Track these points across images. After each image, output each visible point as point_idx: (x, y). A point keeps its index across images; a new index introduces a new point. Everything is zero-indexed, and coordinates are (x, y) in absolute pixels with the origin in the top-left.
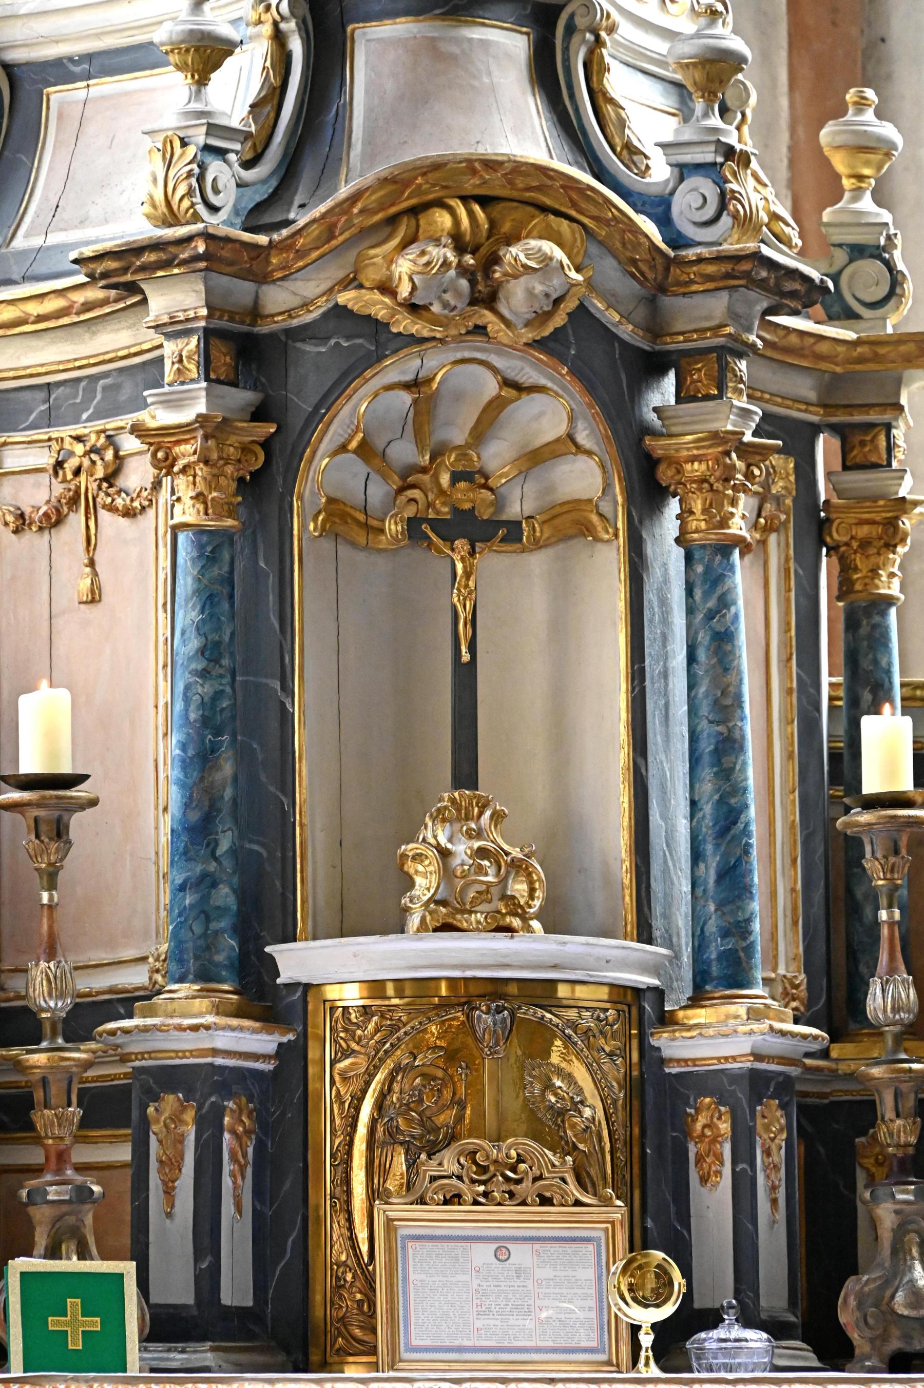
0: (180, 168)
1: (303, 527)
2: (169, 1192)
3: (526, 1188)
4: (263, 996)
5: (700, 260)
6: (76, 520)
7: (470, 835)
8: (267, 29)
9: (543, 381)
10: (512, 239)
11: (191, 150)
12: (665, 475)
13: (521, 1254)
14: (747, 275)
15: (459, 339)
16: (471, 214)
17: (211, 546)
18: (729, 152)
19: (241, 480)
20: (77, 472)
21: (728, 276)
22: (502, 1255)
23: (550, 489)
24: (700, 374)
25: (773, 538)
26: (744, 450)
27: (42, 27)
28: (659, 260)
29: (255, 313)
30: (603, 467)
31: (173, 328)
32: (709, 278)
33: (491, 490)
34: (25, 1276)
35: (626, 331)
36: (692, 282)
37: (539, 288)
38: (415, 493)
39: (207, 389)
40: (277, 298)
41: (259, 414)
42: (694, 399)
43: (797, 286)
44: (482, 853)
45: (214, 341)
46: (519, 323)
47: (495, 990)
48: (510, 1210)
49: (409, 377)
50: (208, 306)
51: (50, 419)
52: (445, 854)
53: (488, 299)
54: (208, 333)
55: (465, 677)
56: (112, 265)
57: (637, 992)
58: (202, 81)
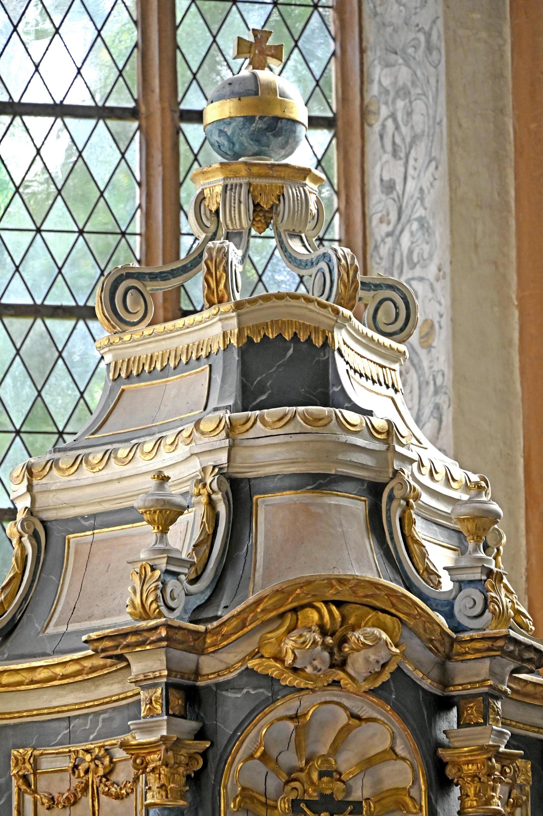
0: (150, 585)
1: (227, 805)
5: (472, 640)
8: (204, 499)
9: (375, 715)
11: (158, 573)
12: (451, 772)
14: (501, 649)
15: (323, 689)
16: (330, 612)
19: (188, 777)
20: (87, 772)
21: (489, 649)
23: (380, 781)
24: (473, 711)
26: (499, 756)
27: (65, 497)
28: (447, 640)
29: (197, 673)
30: (412, 766)
31: (146, 682)
32: (478, 651)
33: (343, 782)
35: (426, 684)
36: (467, 653)
37: (372, 658)
38: (296, 784)
39: (167, 720)
40: (209, 664)
41: (200, 735)
42: (468, 725)
43: (532, 655)
45: (172, 691)
46: (360, 679)
49: (292, 713)
50: (168, 669)
53: (342, 665)
54: (168, 686)
56: (108, 644)
58: (164, 531)
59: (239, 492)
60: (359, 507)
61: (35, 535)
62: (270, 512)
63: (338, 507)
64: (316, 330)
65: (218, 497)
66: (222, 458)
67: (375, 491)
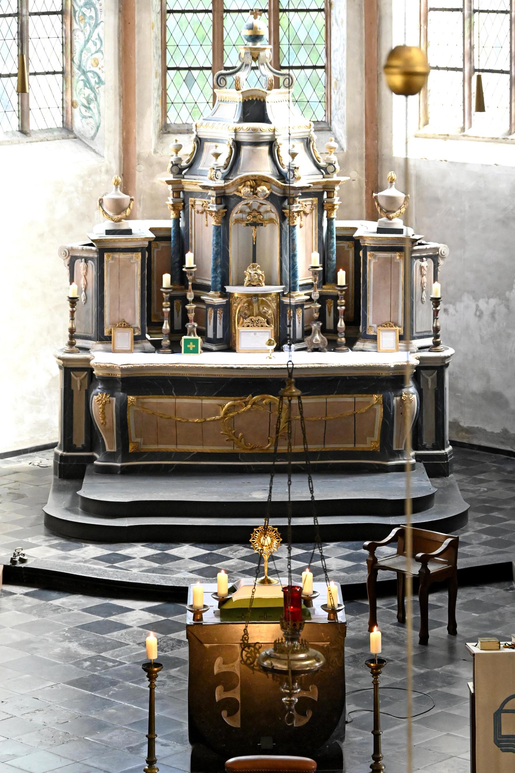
2: (210, 322)
3: (260, 324)
4: (224, 294)
6: (205, 213)
7: (254, 270)
10: (259, 186)
13: (258, 334)
17: (217, 228)
18: (295, 168)
22: (255, 334)
24: (291, 200)
25: (314, 211)
27: (204, 134)
29: (224, 193)
34: (185, 339)
35: (279, 195)
44: (256, 273)
47: (256, 295)
48: (256, 328)
51: (202, 197)
52: (250, 273)
54: (216, 198)
55: (254, 247)
57: (279, 293)
59: (237, 145)
60: (265, 149)
61: (197, 142)
62: (245, 150)
63: (260, 150)
64: (262, 97)
65: (232, 147)
66: (234, 137)
67: (272, 144)
